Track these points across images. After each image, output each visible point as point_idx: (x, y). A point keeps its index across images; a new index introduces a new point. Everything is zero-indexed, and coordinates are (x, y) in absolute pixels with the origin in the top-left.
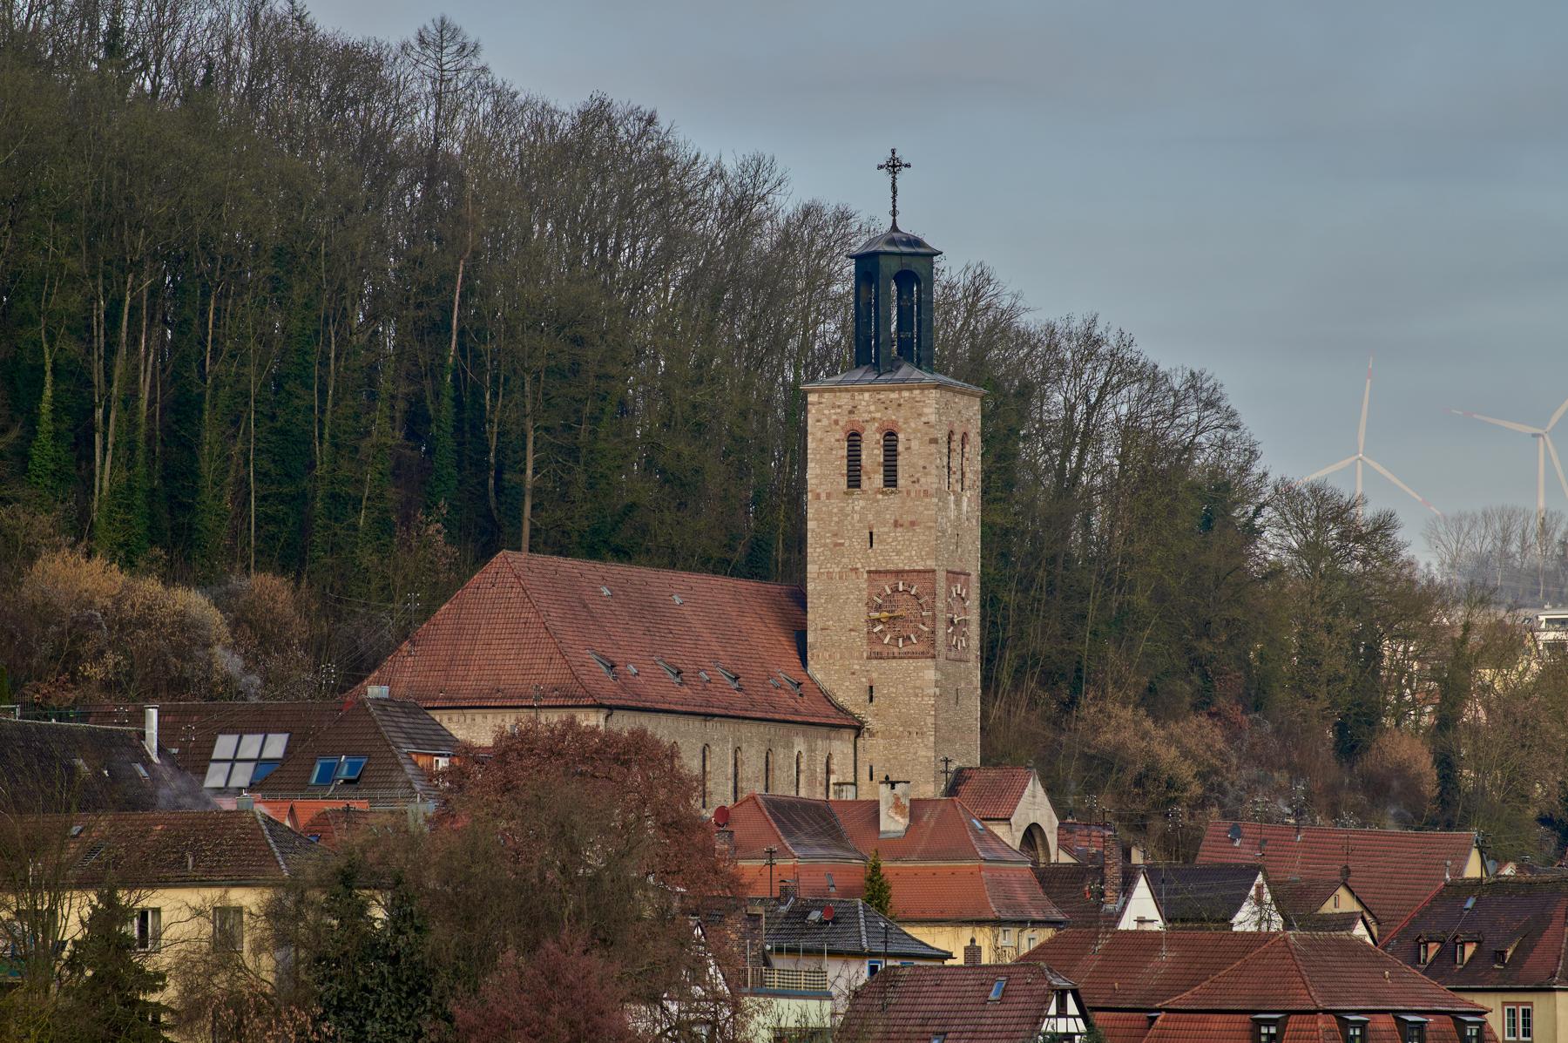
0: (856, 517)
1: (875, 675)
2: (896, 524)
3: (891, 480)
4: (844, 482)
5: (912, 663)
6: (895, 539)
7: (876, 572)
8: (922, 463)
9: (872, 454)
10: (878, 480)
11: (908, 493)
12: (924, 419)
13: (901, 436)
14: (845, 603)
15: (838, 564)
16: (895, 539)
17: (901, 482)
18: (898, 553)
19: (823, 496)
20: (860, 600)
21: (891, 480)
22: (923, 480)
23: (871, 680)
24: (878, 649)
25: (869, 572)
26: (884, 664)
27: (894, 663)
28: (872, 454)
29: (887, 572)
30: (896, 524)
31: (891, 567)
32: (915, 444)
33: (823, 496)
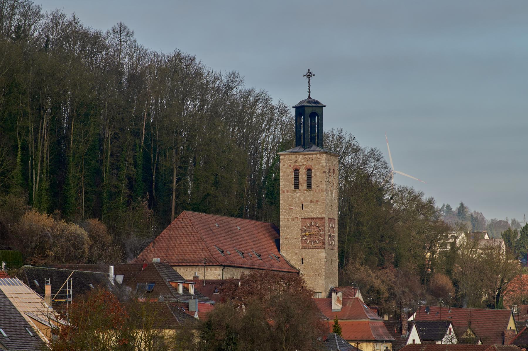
0: (297, 199)
1: (304, 255)
2: (311, 202)
3: (309, 186)
4: (293, 186)
7: (304, 218)
8: (320, 180)
9: (302, 177)
10: (305, 186)
11: (316, 191)
12: (321, 165)
13: (313, 171)
14: (293, 229)
17: (313, 187)
18: (312, 212)
19: (286, 192)
20: (298, 228)
21: (309, 186)
22: (320, 186)
23: (302, 256)
24: (305, 245)
25: (302, 218)
26: (307, 250)
27: (310, 250)
28: (302, 177)
29: (308, 218)
30: (311, 202)
31: (309, 217)
32: (318, 173)
33: (286, 192)
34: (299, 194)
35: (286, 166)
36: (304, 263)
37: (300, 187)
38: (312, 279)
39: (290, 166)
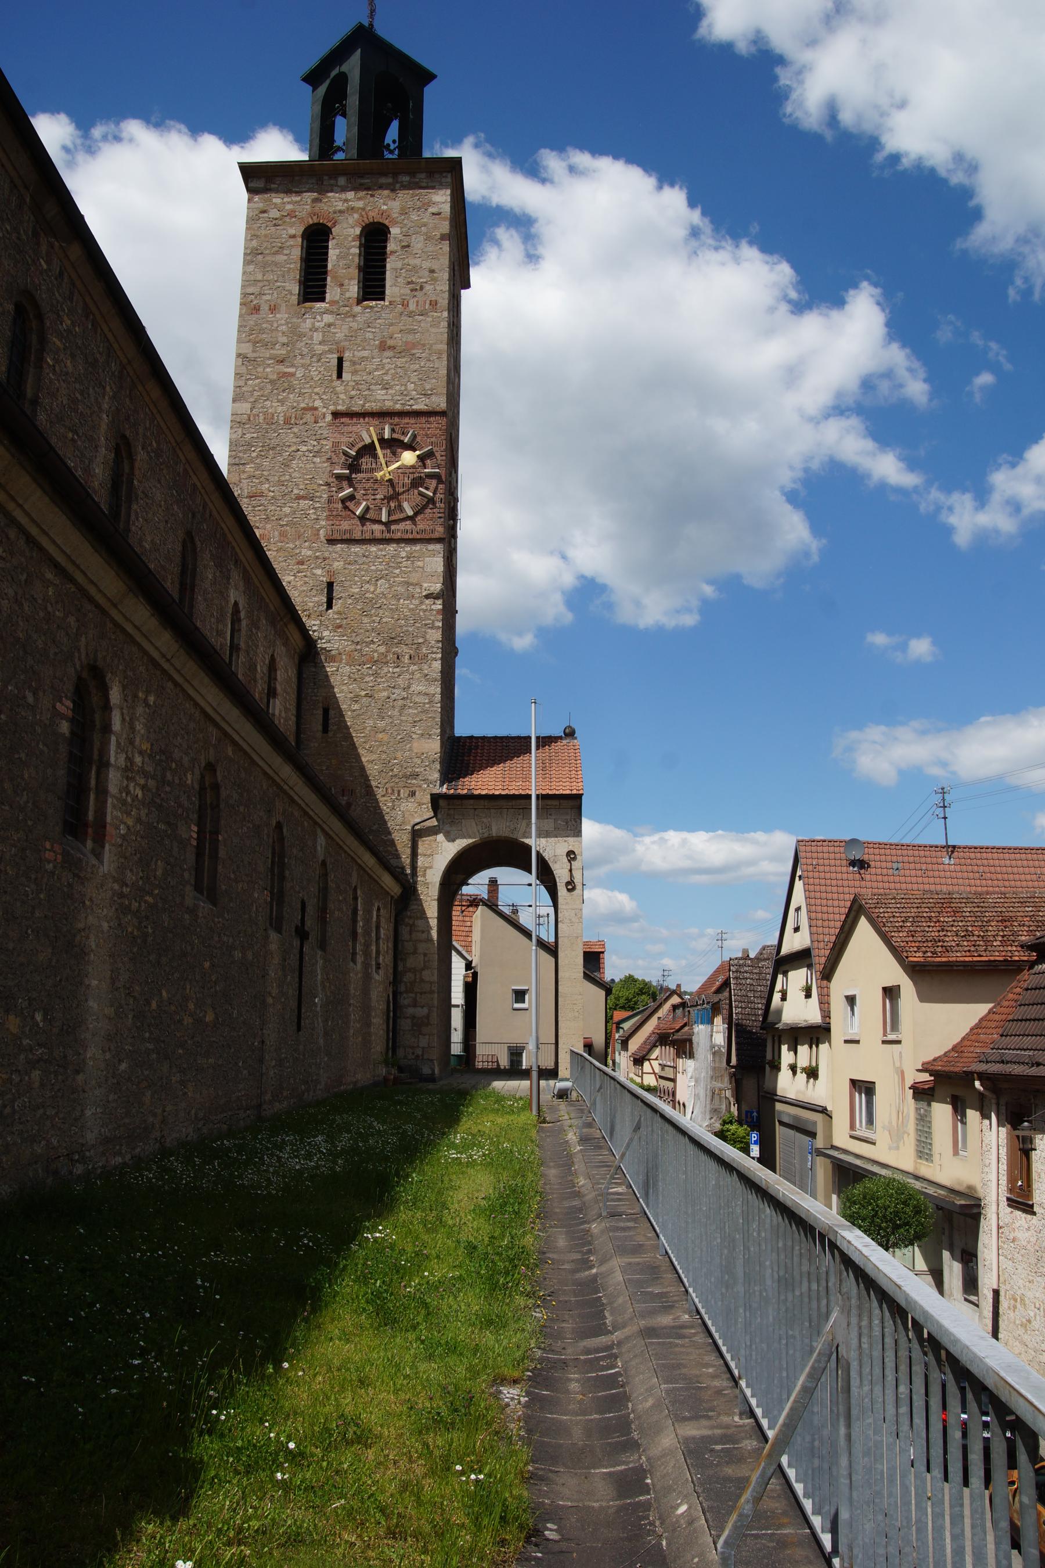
0: (318, 337)
1: (338, 565)
2: (383, 347)
3: (372, 286)
4: (295, 289)
5: (405, 550)
6: (382, 366)
8: (427, 265)
9: (343, 255)
10: (353, 289)
11: (405, 304)
12: (431, 210)
13: (394, 231)
15: (282, 402)
16: (382, 366)
19: (265, 308)
21: (372, 286)
23: (331, 573)
24: (345, 525)
25: (336, 415)
26: (356, 549)
27: (373, 549)
28: (343, 255)
29: (363, 415)
30: (383, 347)
31: (371, 406)
32: (418, 243)
33: (265, 308)
34: (328, 318)
35: (274, 213)
36: (337, 605)
37: (332, 292)
38: (376, 674)
39: (291, 214)
